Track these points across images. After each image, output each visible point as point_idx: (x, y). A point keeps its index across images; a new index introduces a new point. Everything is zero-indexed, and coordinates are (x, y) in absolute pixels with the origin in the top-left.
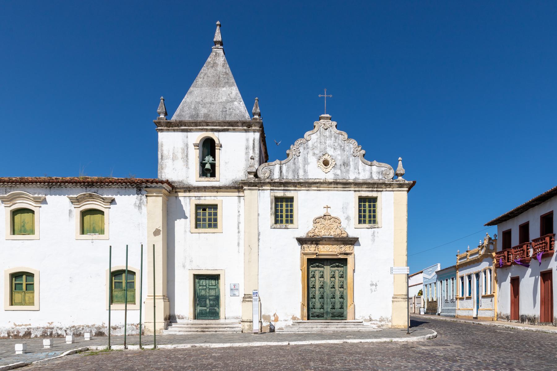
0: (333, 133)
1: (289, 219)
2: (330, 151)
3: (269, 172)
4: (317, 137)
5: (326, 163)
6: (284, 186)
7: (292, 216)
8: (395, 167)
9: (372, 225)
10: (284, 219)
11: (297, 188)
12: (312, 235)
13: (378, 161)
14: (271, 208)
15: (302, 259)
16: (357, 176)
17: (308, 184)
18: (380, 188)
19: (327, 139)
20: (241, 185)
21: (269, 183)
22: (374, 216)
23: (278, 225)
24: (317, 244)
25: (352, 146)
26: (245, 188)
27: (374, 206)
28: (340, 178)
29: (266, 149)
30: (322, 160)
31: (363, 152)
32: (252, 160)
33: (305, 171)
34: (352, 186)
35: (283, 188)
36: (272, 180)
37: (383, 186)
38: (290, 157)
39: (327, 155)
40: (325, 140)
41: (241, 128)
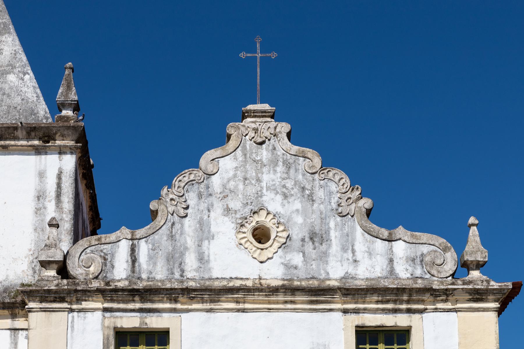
0: (280, 152)
2: (274, 203)
3: (100, 260)
4: (235, 164)
5: (261, 235)
6: (143, 300)
8: (459, 242)
11: (179, 306)
13: (407, 228)
16: (351, 270)
17: (211, 294)
18: (418, 302)
19: (265, 170)
20: (19, 299)
21: (99, 291)
25: (333, 187)
26: (31, 305)
28: (302, 274)
29: (93, 198)
30: (249, 228)
31: (366, 203)
32: (54, 230)
33: (202, 259)
35: (138, 306)
36: (108, 284)
37: (427, 297)
38: (160, 220)
39: (263, 213)
40: (259, 171)
41: (24, 143)
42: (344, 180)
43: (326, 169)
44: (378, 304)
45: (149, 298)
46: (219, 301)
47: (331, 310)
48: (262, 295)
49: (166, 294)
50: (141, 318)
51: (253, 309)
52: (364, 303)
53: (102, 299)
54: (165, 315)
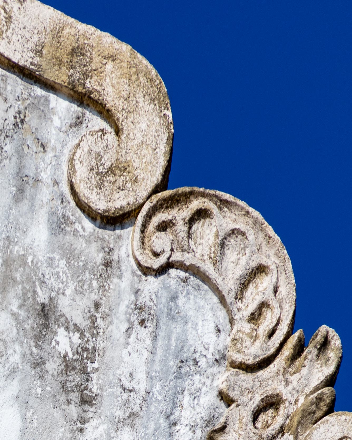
42: (265, 283)
43: (185, 198)
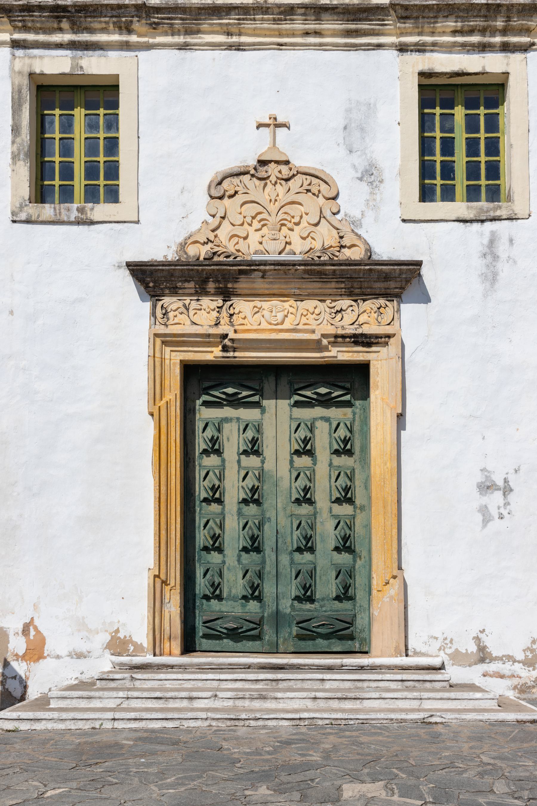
1: (102, 182)
6: (76, 28)
7: (113, 171)
9: (483, 204)
10: (79, 182)
11: (134, 38)
12: (203, 251)
14: (16, 130)
15: (156, 365)
22: (494, 171)
23: (47, 210)
24: (226, 294)
27: (493, 124)
34: (390, 22)
35: (67, 37)
44: (455, 36)
45: (84, 25)
46: (198, 32)
47: (379, 46)
48: (268, 20)
49: (112, 17)
50: (73, 58)
51: (254, 44)
52: (433, 34)
53: (9, 27)
54: (112, 54)
